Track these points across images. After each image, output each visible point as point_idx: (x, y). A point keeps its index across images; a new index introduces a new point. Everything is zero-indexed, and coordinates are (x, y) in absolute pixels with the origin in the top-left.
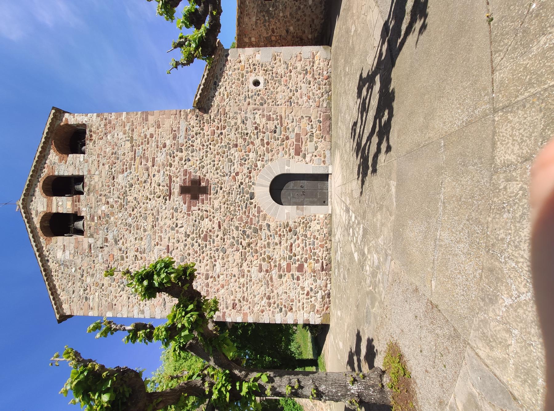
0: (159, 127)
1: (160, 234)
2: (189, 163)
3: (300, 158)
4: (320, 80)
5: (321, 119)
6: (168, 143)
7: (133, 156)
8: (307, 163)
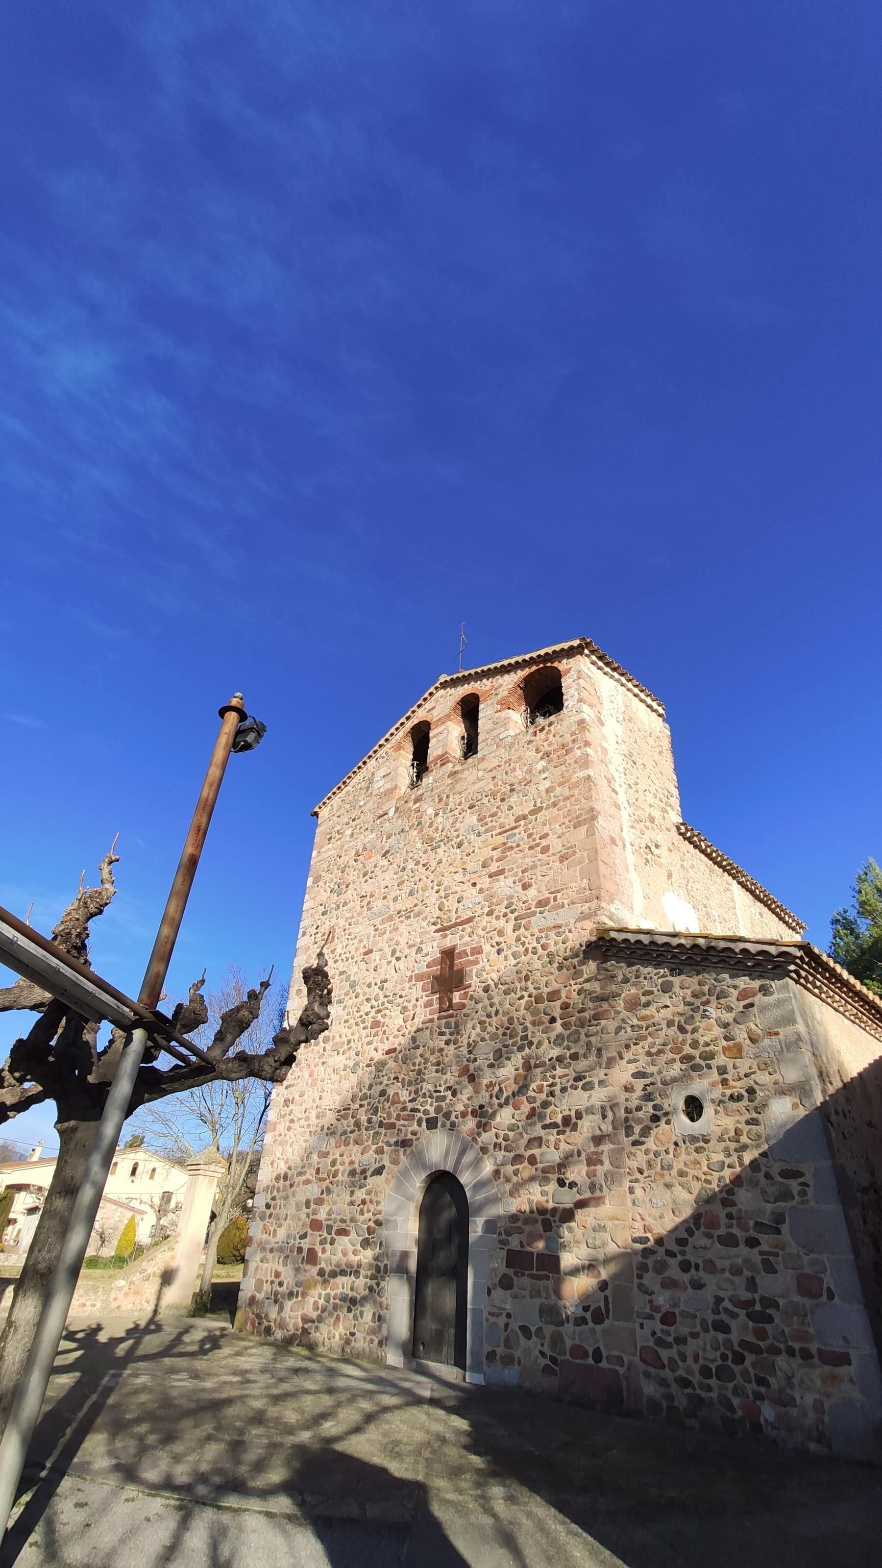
0: (563, 858)
1: (388, 929)
2: (494, 956)
3: (503, 1269)
4: (739, 1380)
5: (604, 1364)
6: (532, 892)
7: (507, 827)
8: (489, 1292)
